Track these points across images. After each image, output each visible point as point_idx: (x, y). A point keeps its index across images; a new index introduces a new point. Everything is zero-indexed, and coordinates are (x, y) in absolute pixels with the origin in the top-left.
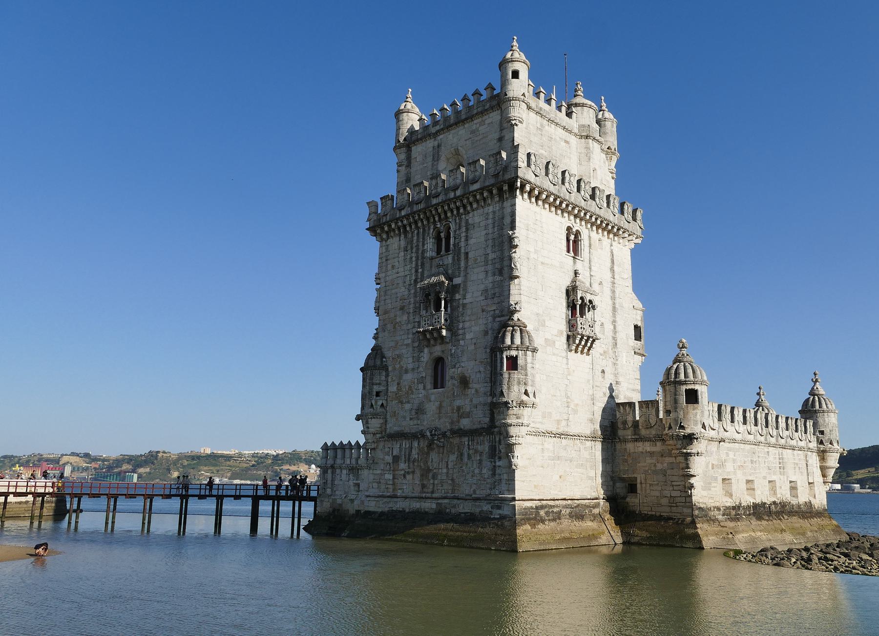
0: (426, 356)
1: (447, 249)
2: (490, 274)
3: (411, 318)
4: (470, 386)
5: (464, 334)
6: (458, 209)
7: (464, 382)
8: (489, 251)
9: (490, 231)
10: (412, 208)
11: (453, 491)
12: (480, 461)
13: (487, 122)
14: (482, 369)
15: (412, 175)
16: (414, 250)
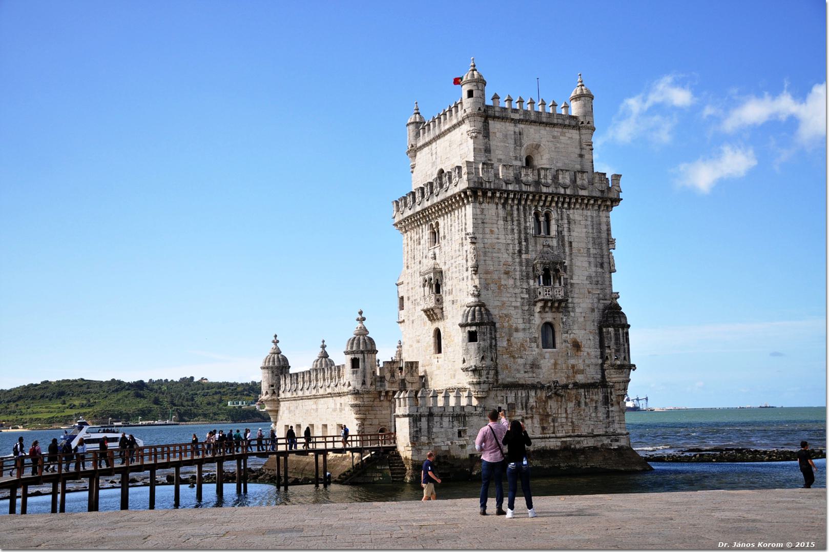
0: (537, 320)
1: (548, 232)
2: (592, 265)
3: (518, 283)
5: (574, 307)
6: (563, 203)
7: (577, 346)
8: (590, 246)
9: (590, 231)
10: (520, 187)
11: (573, 431)
12: (596, 407)
13: (567, 135)
14: (591, 338)
15: (492, 148)
16: (515, 223)
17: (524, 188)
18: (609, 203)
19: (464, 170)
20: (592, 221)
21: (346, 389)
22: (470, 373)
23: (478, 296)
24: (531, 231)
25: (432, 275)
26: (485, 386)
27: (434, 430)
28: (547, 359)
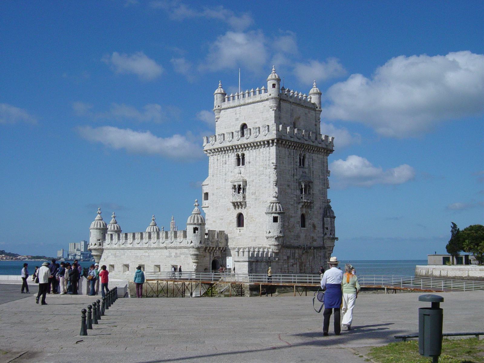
1: (303, 165)
4: (316, 228)
7: (314, 226)
8: (320, 174)
13: (311, 113)
17: (298, 141)
18: (329, 152)
19: (273, 128)
20: (321, 161)
21: (182, 245)
22: (274, 239)
23: (277, 198)
24: (298, 164)
25: (241, 183)
26: (280, 247)
27: (258, 269)
28: (303, 233)
